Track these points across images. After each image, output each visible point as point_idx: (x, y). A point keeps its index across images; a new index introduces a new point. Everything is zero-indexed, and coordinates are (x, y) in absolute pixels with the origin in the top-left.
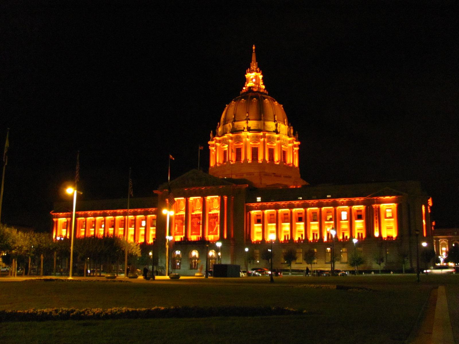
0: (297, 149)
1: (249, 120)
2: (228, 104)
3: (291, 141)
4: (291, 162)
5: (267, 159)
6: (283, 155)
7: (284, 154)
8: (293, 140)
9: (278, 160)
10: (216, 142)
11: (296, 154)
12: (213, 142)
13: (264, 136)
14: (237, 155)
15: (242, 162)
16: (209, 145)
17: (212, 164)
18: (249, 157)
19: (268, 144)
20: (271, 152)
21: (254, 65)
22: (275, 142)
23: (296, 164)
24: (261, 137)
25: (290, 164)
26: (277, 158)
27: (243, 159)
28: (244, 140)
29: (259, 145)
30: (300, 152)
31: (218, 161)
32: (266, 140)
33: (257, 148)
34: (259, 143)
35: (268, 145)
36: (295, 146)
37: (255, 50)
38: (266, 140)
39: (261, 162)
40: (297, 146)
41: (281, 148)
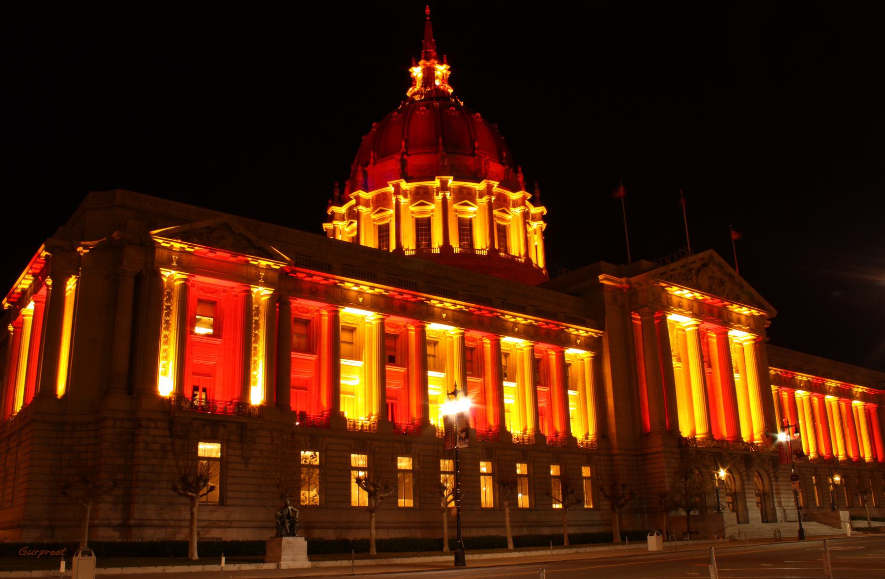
3: (520, 202)
4: (522, 253)
5: (454, 243)
8: (524, 198)
9: (484, 247)
18: (409, 244)
19: (456, 206)
20: (465, 228)
22: (475, 202)
25: (520, 257)
27: (393, 247)
29: (432, 211)
33: (429, 219)
34: (432, 207)
35: (456, 211)
39: (438, 251)
40: (540, 216)
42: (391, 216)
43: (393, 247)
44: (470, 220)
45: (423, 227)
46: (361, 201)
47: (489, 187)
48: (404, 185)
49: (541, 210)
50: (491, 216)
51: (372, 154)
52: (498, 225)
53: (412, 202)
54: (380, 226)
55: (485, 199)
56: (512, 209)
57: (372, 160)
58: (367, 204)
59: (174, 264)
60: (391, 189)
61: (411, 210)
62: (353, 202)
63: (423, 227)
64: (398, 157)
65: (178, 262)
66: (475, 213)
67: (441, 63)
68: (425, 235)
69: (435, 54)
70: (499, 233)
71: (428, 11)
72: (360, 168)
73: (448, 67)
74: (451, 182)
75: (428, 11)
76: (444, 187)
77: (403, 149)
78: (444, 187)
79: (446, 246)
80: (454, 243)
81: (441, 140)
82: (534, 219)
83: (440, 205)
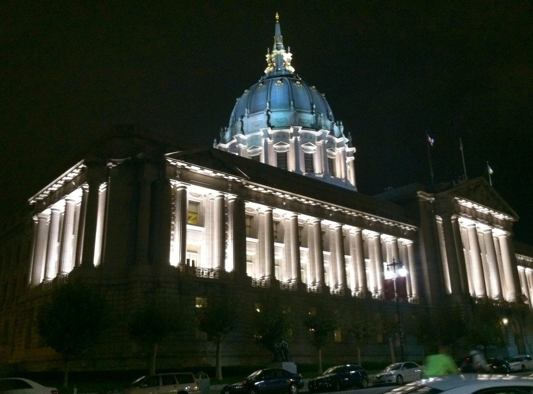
2: (240, 95)
4: (343, 177)
5: (302, 169)
6: (329, 165)
9: (321, 172)
13: (296, 133)
20: (309, 160)
24: (292, 135)
26: (318, 168)
29: (288, 148)
33: (286, 153)
34: (288, 145)
35: (303, 149)
36: (348, 154)
37: (280, 20)
42: (261, 151)
44: (312, 155)
49: (353, 149)
51: (246, 110)
52: (329, 159)
53: (274, 143)
55: (321, 142)
56: (336, 149)
57: (246, 115)
58: (244, 142)
59: (178, 176)
60: (261, 133)
62: (235, 141)
64: (265, 113)
65: (180, 175)
66: (315, 150)
67: (287, 52)
68: (283, 164)
69: (282, 46)
70: (330, 164)
71: (277, 16)
72: (239, 119)
73: (291, 55)
74: (300, 131)
75: (277, 16)
77: (268, 108)
78: (296, 133)
81: (292, 103)
82: (348, 154)
83: (293, 145)
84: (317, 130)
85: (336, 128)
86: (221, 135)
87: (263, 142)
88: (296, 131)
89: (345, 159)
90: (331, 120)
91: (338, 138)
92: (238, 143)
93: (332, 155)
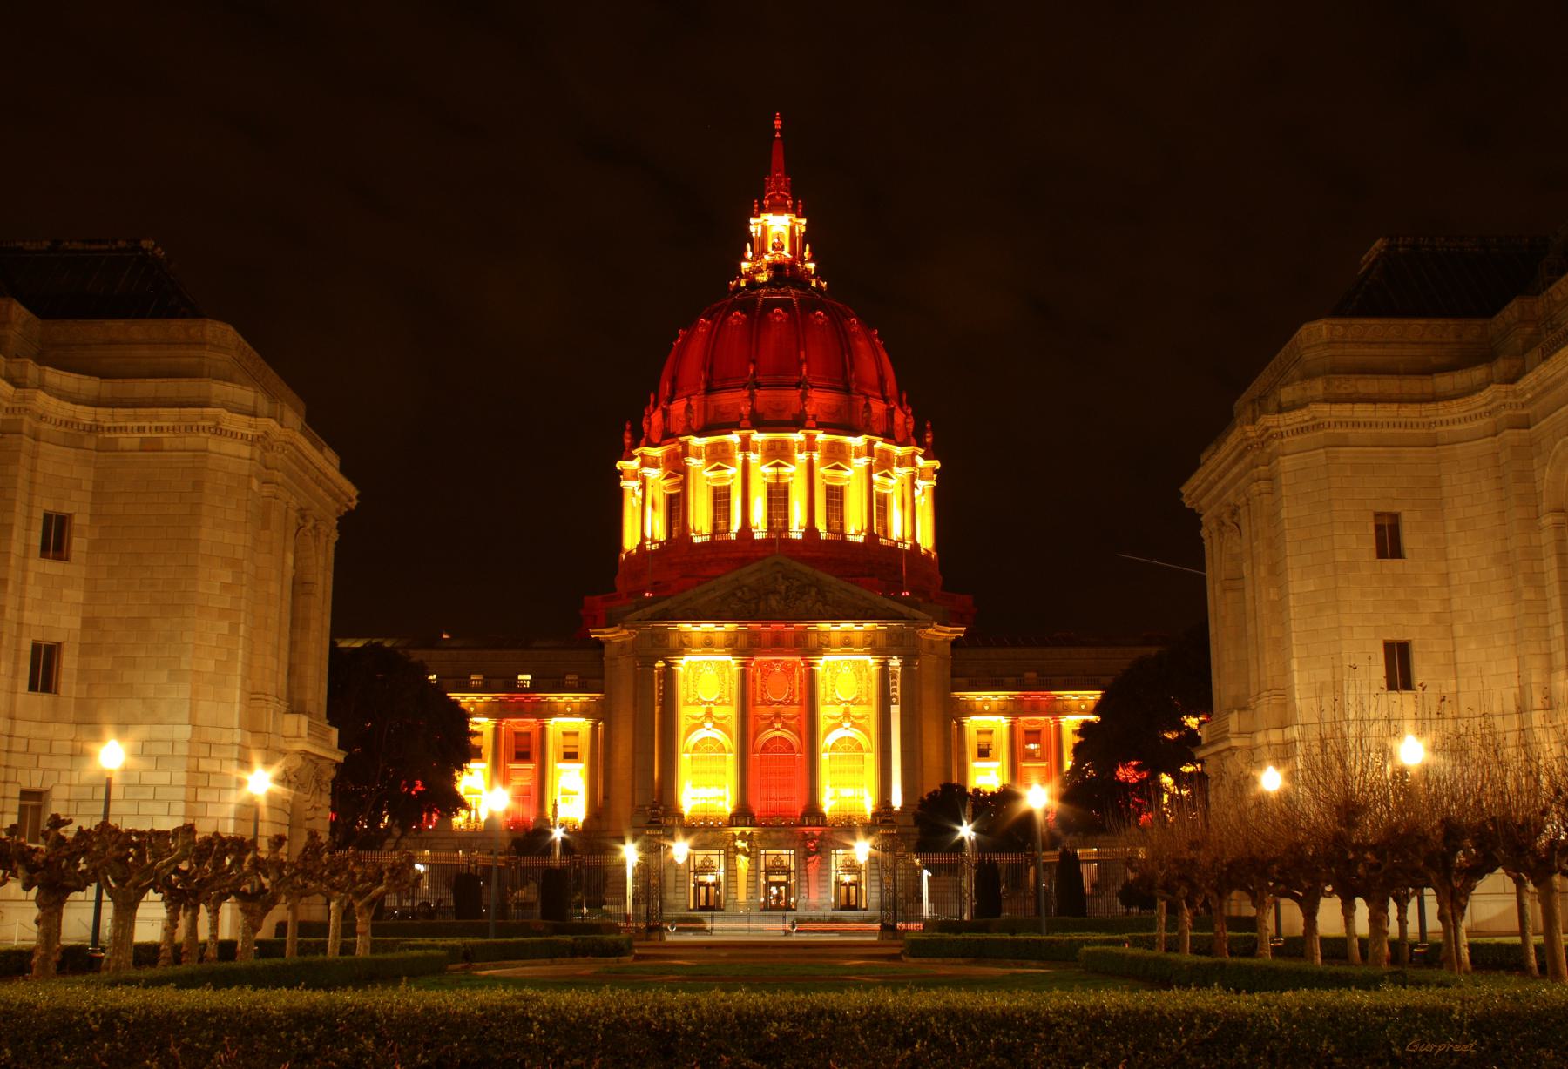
0: (926, 485)
1: (758, 386)
4: (908, 534)
7: (878, 506)
8: (914, 454)
10: (643, 465)
11: (925, 503)
12: (634, 464)
14: (715, 511)
15: (733, 537)
16: (621, 472)
17: (630, 541)
20: (836, 496)
21: (777, 184)
23: (926, 540)
28: (739, 457)
30: (939, 496)
31: (648, 535)
32: (817, 456)
38: (817, 456)
39: (800, 536)
41: (871, 483)
43: (736, 525)
45: (778, 496)
46: (691, 450)
47: (870, 444)
48: (757, 437)
49: (937, 464)
50: (871, 483)
52: (878, 494)
54: (715, 489)
61: (762, 474)
63: (778, 496)
64: (746, 393)
70: (878, 506)
76: (810, 446)
78: (810, 446)
79: (811, 530)
80: (821, 525)
84: (856, 433)
85: (899, 417)
86: (646, 427)
87: (739, 457)
88: (810, 438)
89: (914, 486)
90: (885, 400)
91: (901, 445)
92: (686, 454)
93: (883, 486)
